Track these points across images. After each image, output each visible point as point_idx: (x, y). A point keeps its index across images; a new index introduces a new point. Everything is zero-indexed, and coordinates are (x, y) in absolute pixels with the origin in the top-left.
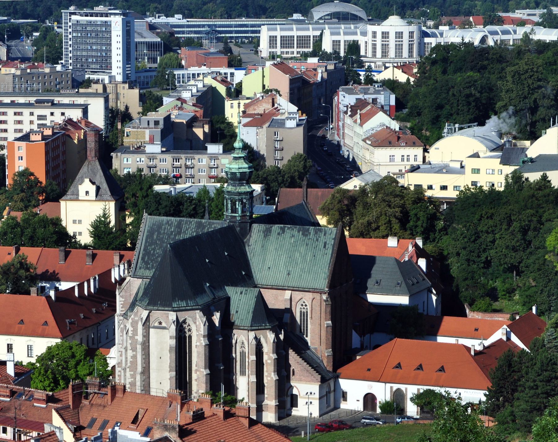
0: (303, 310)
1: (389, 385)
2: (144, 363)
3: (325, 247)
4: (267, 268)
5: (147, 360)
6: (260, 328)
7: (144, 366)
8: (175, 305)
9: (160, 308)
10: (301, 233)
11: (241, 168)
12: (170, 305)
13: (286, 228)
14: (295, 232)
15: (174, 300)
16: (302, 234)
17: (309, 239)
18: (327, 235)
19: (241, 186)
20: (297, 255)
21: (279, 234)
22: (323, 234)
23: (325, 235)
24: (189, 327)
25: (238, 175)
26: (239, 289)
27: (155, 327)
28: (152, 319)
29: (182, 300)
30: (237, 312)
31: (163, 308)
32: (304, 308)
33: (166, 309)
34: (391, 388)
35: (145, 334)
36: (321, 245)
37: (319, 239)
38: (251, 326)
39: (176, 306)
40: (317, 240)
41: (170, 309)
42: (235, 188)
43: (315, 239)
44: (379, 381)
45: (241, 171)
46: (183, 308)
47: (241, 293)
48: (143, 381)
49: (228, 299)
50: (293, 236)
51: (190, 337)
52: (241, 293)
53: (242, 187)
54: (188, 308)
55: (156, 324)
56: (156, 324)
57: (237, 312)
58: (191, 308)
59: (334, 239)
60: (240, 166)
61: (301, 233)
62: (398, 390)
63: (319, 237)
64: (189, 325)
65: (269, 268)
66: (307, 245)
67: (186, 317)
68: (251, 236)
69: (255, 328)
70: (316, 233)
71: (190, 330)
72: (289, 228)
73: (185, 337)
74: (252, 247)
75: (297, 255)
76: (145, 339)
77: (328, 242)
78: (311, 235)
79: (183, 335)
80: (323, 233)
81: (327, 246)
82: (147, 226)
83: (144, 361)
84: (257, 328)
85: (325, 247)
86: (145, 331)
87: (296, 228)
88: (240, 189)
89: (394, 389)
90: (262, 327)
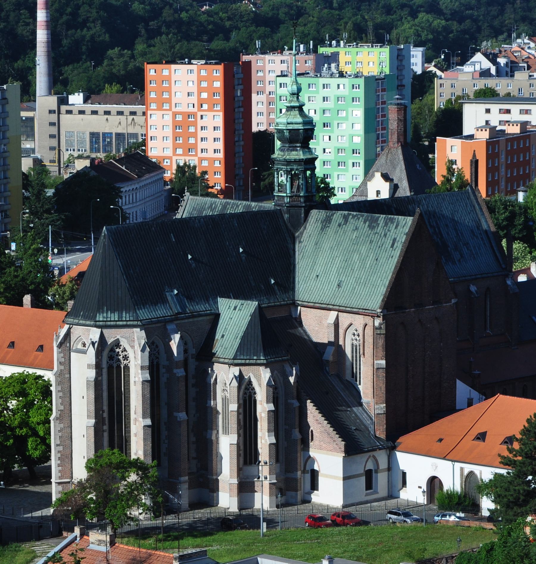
0: (355, 342)
1: (458, 465)
2: (62, 404)
3: (392, 246)
4: (315, 276)
5: (68, 399)
6: (247, 361)
7: (62, 408)
8: (100, 317)
9: (81, 322)
10: (367, 223)
11: (292, 123)
12: (93, 318)
13: (351, 217)
14: (360, 223)
15: (100, 309)
16: (369, 226)
17: (376, 233)
18: (399, 227)
19: (291, 151)
20: (356, 257)
21: (339, 225)
22: (394, 226)
23: (396, 227)
24: (124, 353)
25: (287, 134)
26: (234, 302)
27: (78, 351)
28: (73, 338)
29: (113, 311)
30: (223, 336)
31: (84, 322)
32: (356, 340)
33: (88, 323)
34: (462, 469)
35: (63, 360)
36: (389, 242)
37: (388, 233)
38: (234, 359)
39: (101, 319)
40: (385, 235)
41: (92, 323)
42: (282, 153)
43: (382, 235)
44: (444, 458)
45: (290, 127)
46: (112, 323)
47: (235, 308)
48: (59, 431)
49: (217, 316)
50: (357, 229)
51: (127, 368)
52: (235, 308)
53: (294, 153)
54: (121, 323)
55: (80, 346)
56: (80, 346)
57: (223, 336)
58: (125, 323)
59: (407, 234)
60: (290, 120)
61: (367, 223)
62: (471, 473)
63: (389, 230)
64: (125, 350)
65: (318, 276)
66: (371, 242)
67: (118, 337)
68: (305, 228)
69: (240, 361)
70: (386, 224)
71: (126, 358)
72: (354, 217)
73: (119, 367)
74: (303, 244)
75: (356, 257)
76: (62, 367)
77: (397, 239)
78: (379, 228)
79: (115, 365)
80: (395, 224)
81: (396, 244)
82: (186, 212)
83: (60, 401)
84: (243, 361)
85: (392, 246)
86: (62, 355)
87: (363, 216)
88: (289, 155)
89: (466, 472)
90: (251, 361)
